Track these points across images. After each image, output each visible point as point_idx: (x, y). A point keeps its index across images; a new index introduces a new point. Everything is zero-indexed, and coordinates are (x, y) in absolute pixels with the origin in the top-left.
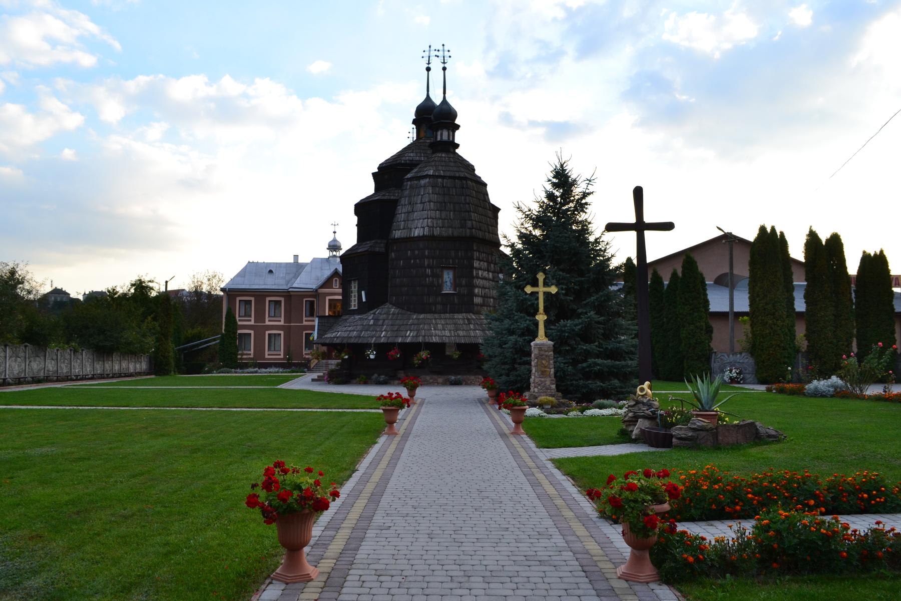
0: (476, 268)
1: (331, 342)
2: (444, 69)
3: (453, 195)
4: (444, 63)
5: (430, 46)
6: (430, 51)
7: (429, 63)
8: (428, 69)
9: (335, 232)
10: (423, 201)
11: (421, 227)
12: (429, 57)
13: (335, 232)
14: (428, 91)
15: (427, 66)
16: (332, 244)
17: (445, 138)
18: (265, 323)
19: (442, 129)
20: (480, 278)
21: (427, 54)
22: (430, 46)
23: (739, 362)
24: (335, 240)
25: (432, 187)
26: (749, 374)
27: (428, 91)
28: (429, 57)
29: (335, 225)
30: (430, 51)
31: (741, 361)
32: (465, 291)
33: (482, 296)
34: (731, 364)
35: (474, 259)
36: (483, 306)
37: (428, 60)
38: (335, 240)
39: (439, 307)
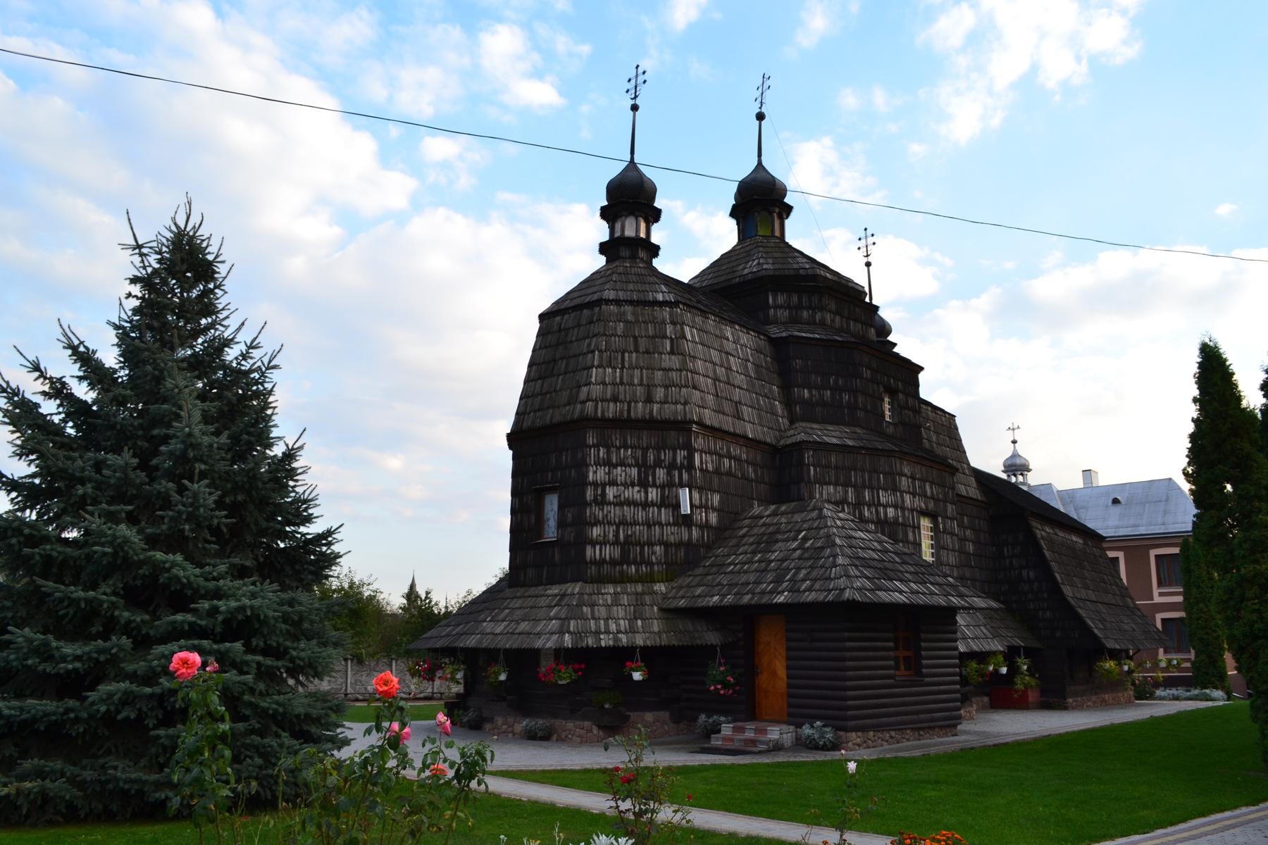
0: (595, 484)
3: (571, 342)
4: (636, 97)
8: (760, 117)
9: (1014, 442)
13: (1014, 442)
14: (760, 155)
16: (1009, 462)
17: (630, 232)
18: (1152, 600)
20: (610, 503)
24: (1015, 455)
27: (760, 155)
29: (1013, 429)
32: (572, 535)
33: (616, 542)
35: (587, 466)
36: (621, 564)
38: (1015, 455)
39: (531, 572)
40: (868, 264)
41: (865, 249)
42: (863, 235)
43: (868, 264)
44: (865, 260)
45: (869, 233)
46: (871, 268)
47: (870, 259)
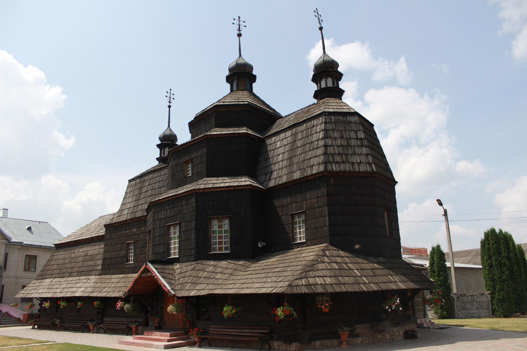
1: (311, 291)
2: (321, 29)
5: (239, 18)
6: (239, 21)
7: (239, 30)
10: (359, 136)
11: (366, 163)
12: (239, 25)
15: (238, 32)
19: (326, 78)
21: (236, 22)
22: (239, 18)
23: (476, 301)
25: (362, 125)
26: (485, 309)
28: (239, 25)
30: (239, 21)
31: (478, 300)
34: (471, 303)
37: (238, 27)
40: (170, 107)
41: (169, 99)
42: (169, 91)
43: (170, 107)
44: (168, 104)
45: (172, 93)
46: (171, 108)
47: (171, 104)
